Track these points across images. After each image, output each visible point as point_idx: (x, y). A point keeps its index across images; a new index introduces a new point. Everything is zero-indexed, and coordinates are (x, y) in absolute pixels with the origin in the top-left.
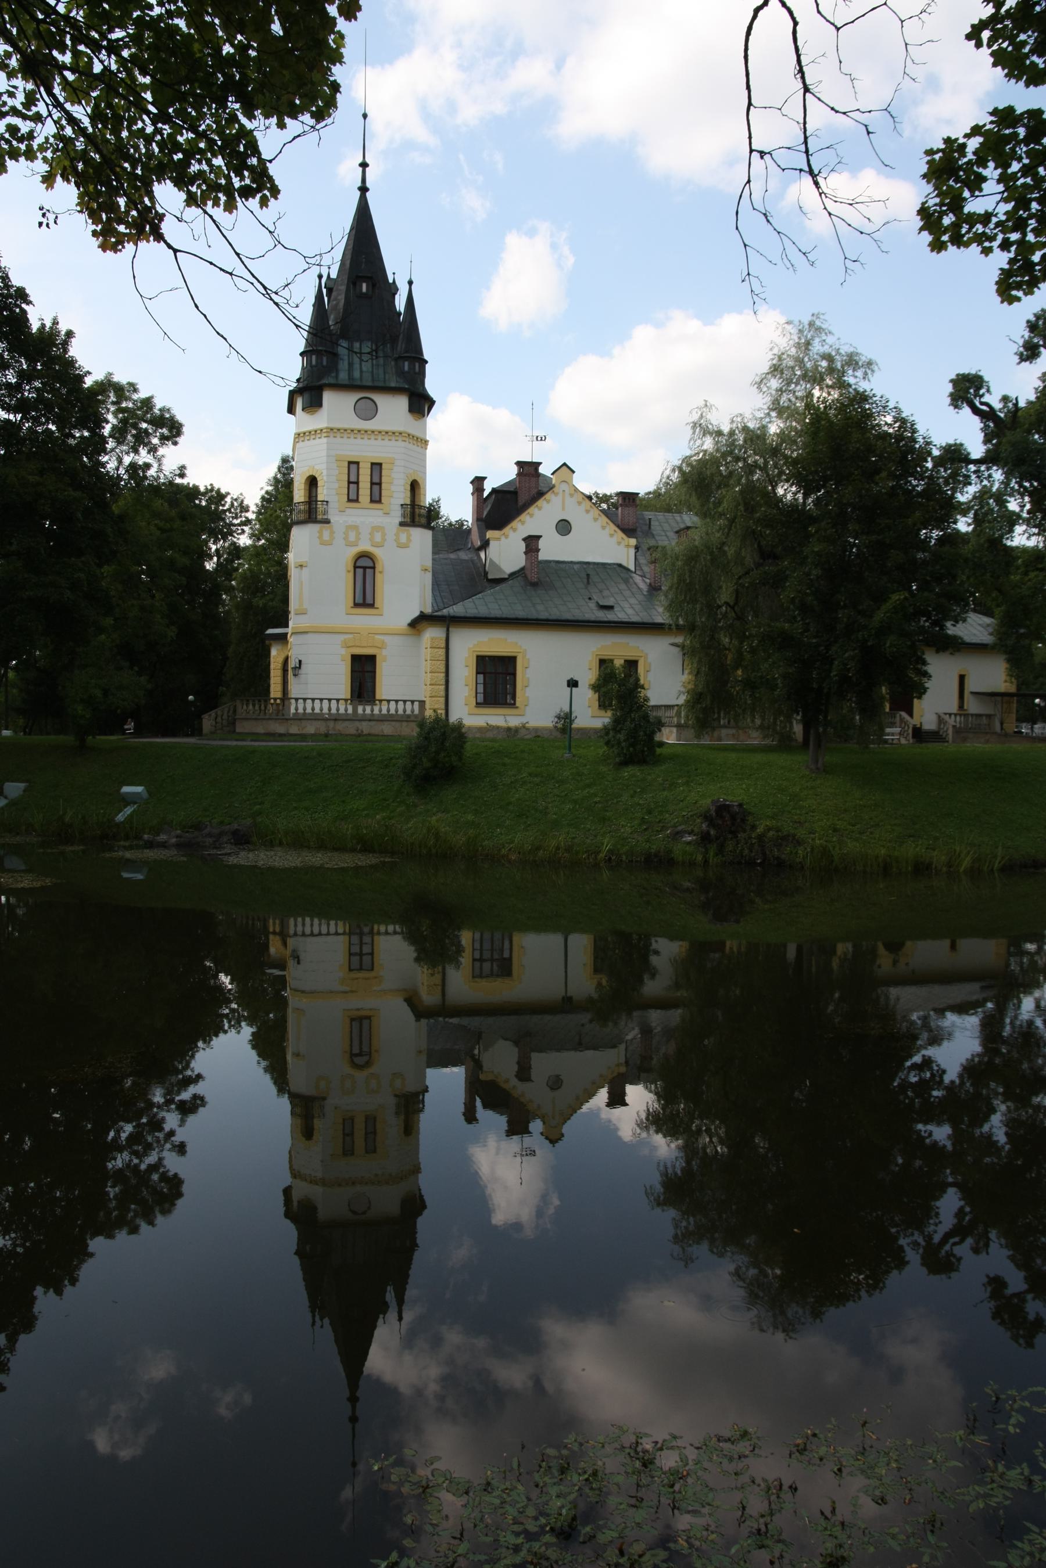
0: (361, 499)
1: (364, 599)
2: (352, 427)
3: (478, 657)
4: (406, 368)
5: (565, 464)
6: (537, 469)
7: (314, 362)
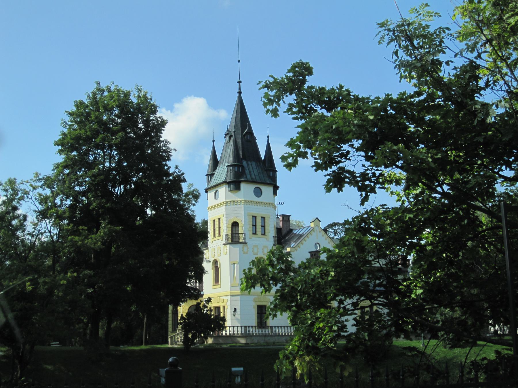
0: (257, 233)
2: (254, 200)
4: (271, 175)
5: (317, 218)
6: (289, 219)
7: (236, 170)
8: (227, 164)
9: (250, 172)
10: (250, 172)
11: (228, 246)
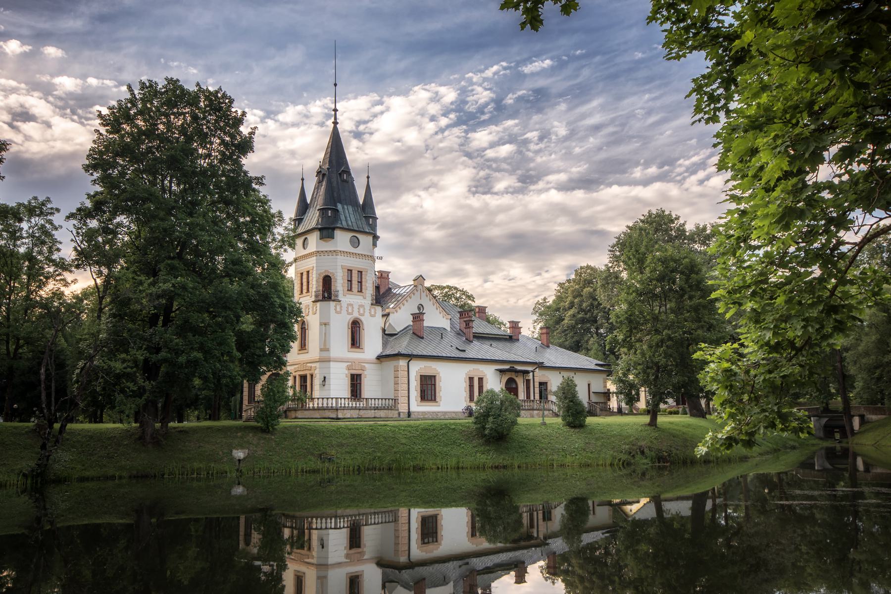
1: (355, 342)
3: (421, 376)
8: (318, 207)
9: (346, 217)
10: (346, 217)
11: (318, 304)
